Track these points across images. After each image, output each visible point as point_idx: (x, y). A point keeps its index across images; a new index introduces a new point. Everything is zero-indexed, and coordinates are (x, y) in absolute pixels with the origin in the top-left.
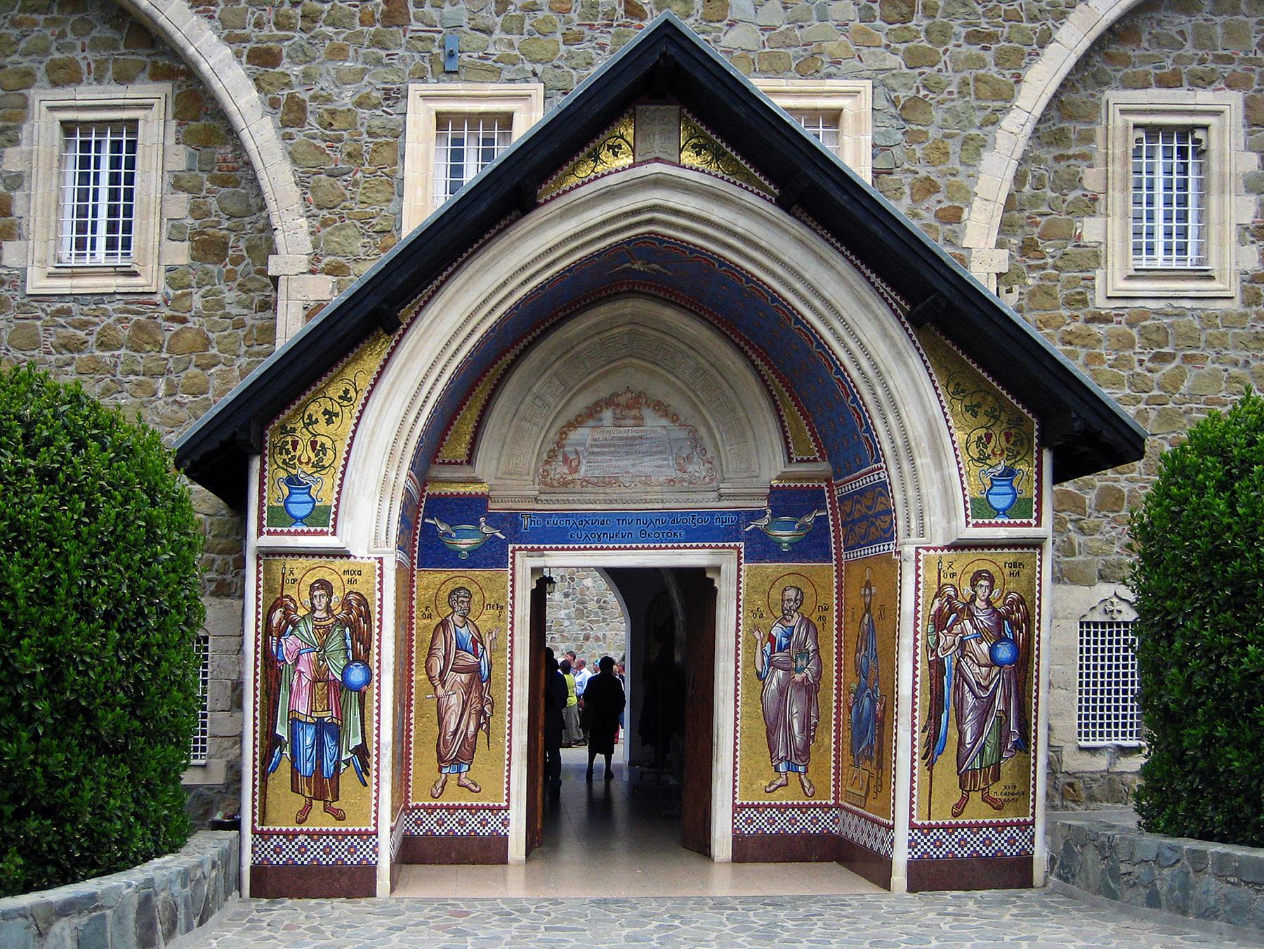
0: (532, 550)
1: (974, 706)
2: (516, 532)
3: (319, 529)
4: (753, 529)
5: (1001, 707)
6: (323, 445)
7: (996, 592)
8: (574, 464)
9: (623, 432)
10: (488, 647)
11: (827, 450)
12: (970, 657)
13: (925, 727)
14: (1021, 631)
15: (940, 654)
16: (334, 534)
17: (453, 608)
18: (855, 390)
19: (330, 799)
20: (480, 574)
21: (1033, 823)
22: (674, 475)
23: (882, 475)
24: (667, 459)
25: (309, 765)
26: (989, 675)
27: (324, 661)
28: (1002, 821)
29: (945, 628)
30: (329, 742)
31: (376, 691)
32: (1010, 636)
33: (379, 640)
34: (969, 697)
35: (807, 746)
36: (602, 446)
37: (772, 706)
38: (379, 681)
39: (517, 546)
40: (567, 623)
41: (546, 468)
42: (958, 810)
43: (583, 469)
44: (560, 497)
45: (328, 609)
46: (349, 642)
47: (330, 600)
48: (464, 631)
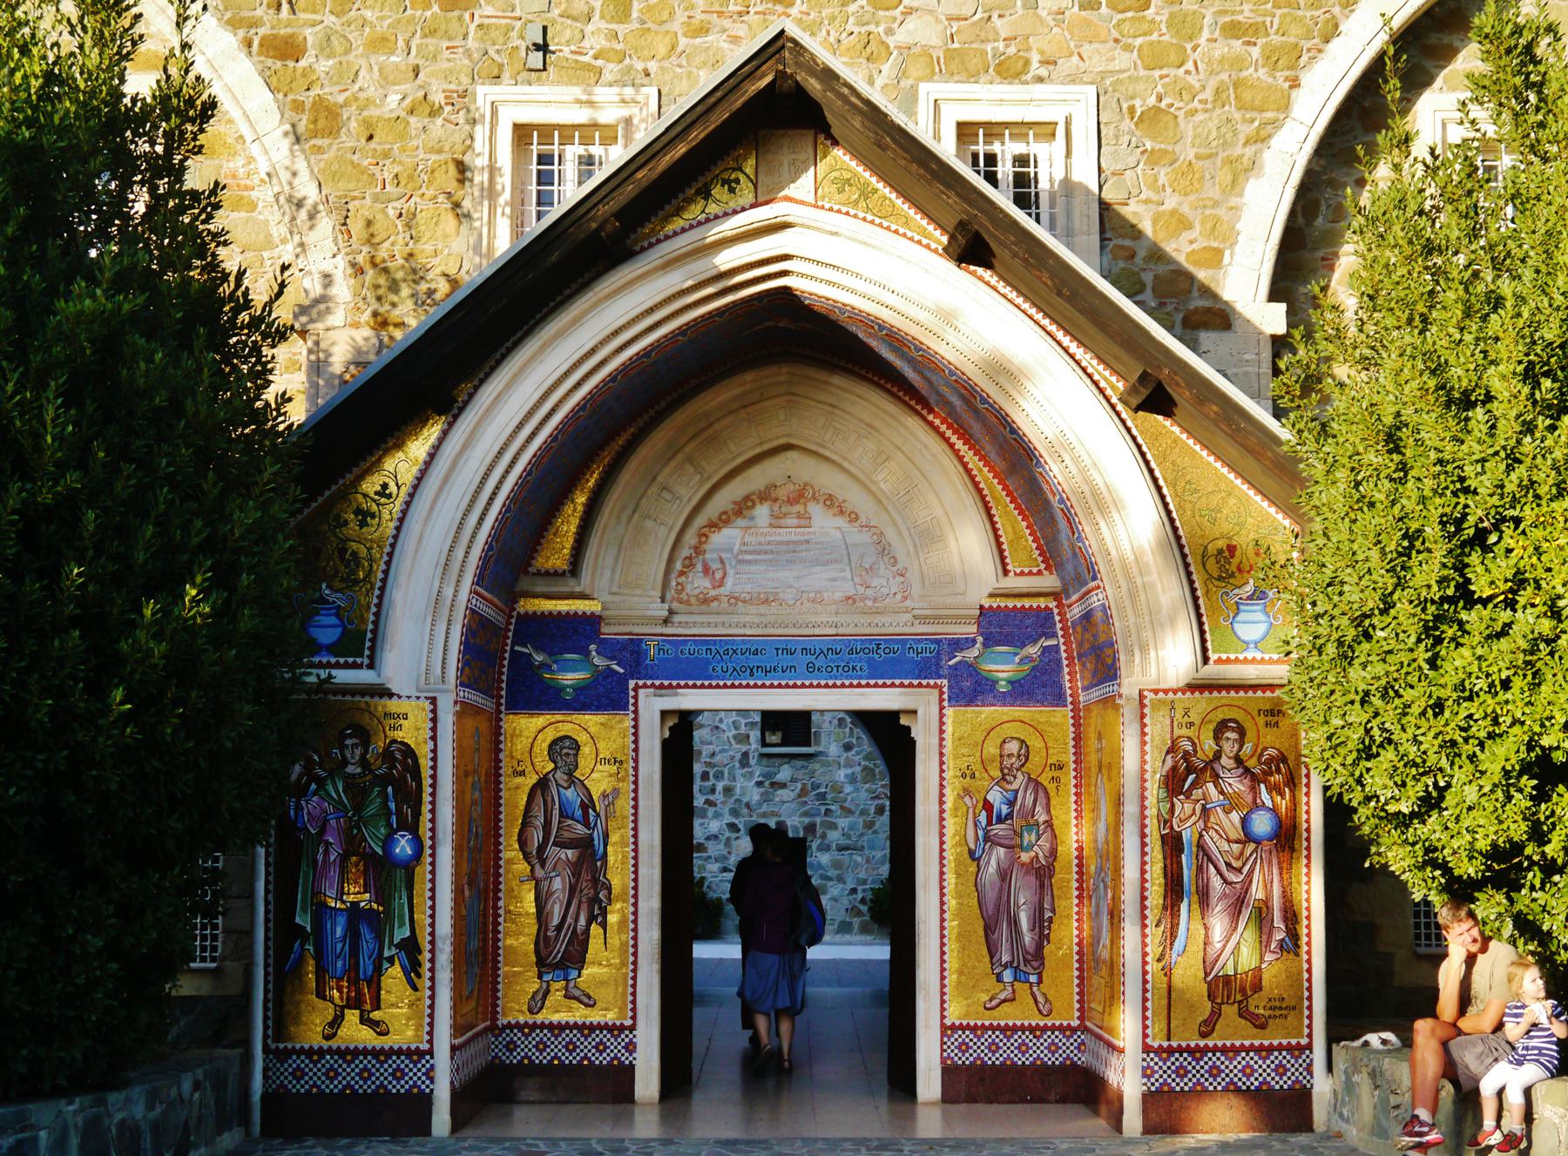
0: (662, 687)
1: (1225, 895)
2: (638, 663)
3: (351, 660)
4: (960, 662)
5: (1260, 895)
6: (355, 554)
7: (1248, 748)
8: (718, 575)
9: (783, 535)
10: (602, 814)
11: (1050, 556)
14: (1283, 797)
15: (1175, 827)
16: (371, 666)
17: (554, 762)
19: (368, 1007)
20: (592, 720)
21: (1309, 1047)
22: (852, 592)
24: (843, 570)
25: (340, 964)
26: (1242, 853)
27: (360, 829)
28: (1266, 1043)
29: (1181, 793)
30: (366, 934)
31: (429, 868)
32: (1269, 803)
33: (433, 803)
34: (1216, 882)
35: (1040, 947)
36: (758, 553)
37: (991, 896)
38: (433, 855)
39: (641, 683)
40: (848, 789)
41: (680, 580)
42: (1207, 1029)
43: (729, 581)
44: (699, 619)
45: (363, 762)
46: (392, 806)
47: (366, 752)
48: (570, 793)
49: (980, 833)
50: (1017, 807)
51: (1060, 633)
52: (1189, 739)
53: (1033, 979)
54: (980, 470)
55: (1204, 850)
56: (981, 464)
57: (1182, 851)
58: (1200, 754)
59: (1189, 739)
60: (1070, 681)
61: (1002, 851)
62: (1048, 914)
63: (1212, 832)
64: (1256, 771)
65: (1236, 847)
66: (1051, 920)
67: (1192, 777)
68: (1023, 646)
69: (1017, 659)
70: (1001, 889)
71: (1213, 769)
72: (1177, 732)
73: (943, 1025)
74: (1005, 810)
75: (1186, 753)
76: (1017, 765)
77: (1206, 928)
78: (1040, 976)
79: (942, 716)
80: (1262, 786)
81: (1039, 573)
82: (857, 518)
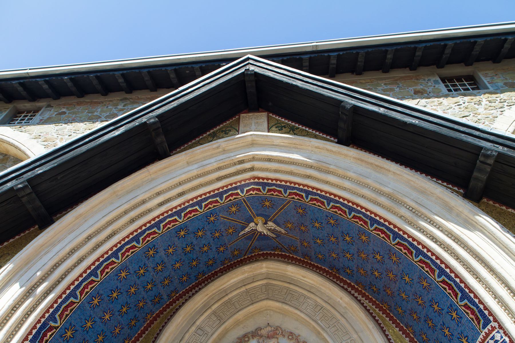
18: (438, 262)
54: (374, 310)
56: (374, 307)
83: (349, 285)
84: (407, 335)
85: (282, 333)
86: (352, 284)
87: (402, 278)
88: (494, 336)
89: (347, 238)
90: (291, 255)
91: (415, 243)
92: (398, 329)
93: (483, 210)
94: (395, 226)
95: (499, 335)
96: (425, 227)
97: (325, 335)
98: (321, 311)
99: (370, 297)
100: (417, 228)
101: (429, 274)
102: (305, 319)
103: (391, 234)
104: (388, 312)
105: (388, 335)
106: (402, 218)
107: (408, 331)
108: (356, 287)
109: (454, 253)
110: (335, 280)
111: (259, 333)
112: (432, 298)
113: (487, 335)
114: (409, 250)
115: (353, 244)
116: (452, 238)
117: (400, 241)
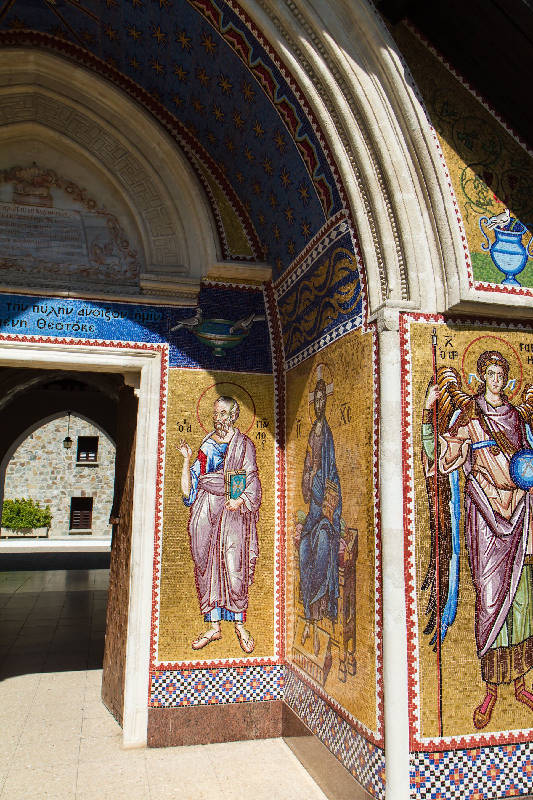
9: (25, 210)
12: (484, 475)
13: (426, 581)
15: (441, 468)
18: (306, 110)
22: (88, 266)
23: (343, 227)
24: (80, 247)
26: (510, 502)
29: (447, 430)
34: (485, 535)
49: (194, 481)
50: (228, 459)
51: (268, 312)
52: (453, 370)
53: (238, 617)
54: (205, 172)
55: (472, 497)
57: (448, 497)
58: (465, 389)
59: (453, 370)
60: (275, 352)
61: (213, 497)
62: (252, 556)
63: (479, 477)
64: (521, 409)
65: (505, 494)
66: (255, 562)
67: (457, 413)
68: (237, 319)
69: (231, 330)
70: (211, 532)
71: (477, 404)
72: (440, 362)
73: (151, 666)
74: (217, 460)
75: (450, 384)
76: (228, 421)
77: (478, 589)
78: (244, 613)
79: (163, 375)
80: (527, 426)
81: (252, 260)
82: (95, 206)
83: (176, 125)
84: (242, 214)
85: (57, 181)
86: (181, 125)
87: (252, 127)
88: (339, 226)
89: (183, 39)
90: (85, 51)
91: (283, 72)
92: (231, 203)
93: (395, 39)
94: (261, 35)
95: (345, 225)
96: (304, 47)
97: (124, 195)
98: (123, 158)
99: (204, 150)
100: (293, 45)
101: (289, 128)
102: (96, 167)
103: (251, 48)
104: (224, 177)
105: (216, 209)
106: (276, 20)
107: (244, 209)
108: (186, 130)
109: (331, 102)
110: (154, 112)
111: (18, 176)
112: (284, 166)
113: (333, 223)
114: (271, 82)
115: (190, 53)
116: (337, 76)
117: (262, 63)
